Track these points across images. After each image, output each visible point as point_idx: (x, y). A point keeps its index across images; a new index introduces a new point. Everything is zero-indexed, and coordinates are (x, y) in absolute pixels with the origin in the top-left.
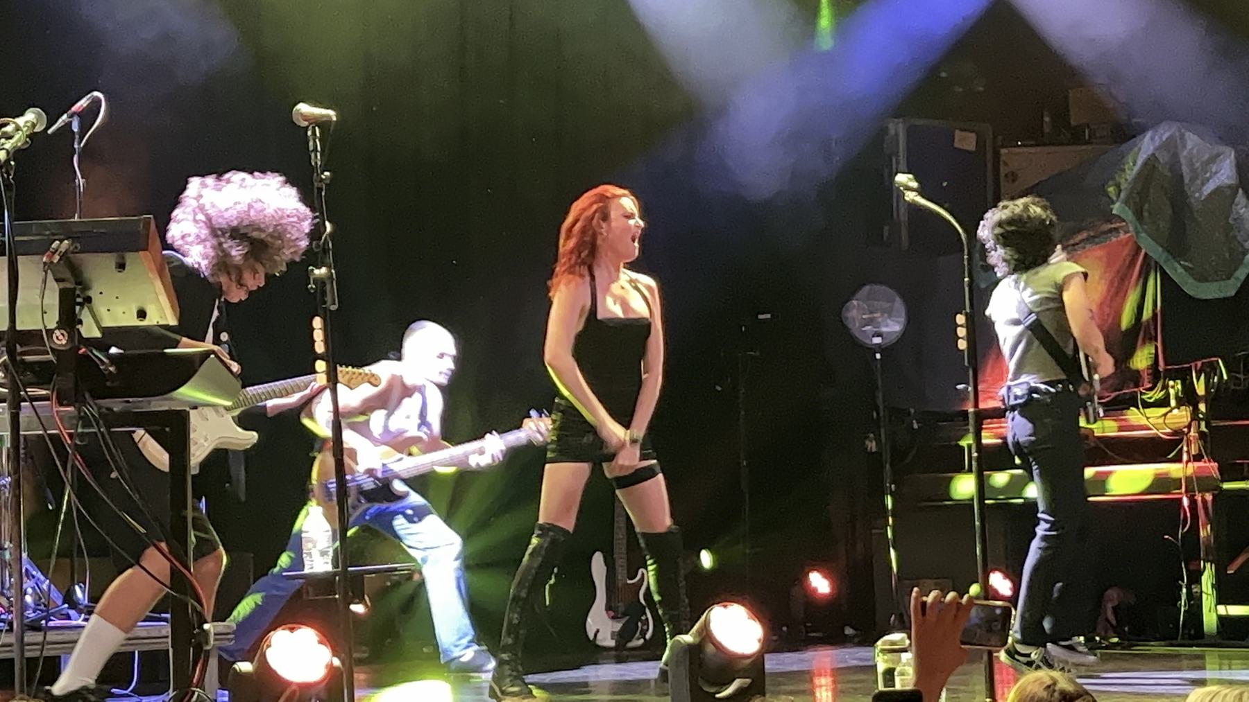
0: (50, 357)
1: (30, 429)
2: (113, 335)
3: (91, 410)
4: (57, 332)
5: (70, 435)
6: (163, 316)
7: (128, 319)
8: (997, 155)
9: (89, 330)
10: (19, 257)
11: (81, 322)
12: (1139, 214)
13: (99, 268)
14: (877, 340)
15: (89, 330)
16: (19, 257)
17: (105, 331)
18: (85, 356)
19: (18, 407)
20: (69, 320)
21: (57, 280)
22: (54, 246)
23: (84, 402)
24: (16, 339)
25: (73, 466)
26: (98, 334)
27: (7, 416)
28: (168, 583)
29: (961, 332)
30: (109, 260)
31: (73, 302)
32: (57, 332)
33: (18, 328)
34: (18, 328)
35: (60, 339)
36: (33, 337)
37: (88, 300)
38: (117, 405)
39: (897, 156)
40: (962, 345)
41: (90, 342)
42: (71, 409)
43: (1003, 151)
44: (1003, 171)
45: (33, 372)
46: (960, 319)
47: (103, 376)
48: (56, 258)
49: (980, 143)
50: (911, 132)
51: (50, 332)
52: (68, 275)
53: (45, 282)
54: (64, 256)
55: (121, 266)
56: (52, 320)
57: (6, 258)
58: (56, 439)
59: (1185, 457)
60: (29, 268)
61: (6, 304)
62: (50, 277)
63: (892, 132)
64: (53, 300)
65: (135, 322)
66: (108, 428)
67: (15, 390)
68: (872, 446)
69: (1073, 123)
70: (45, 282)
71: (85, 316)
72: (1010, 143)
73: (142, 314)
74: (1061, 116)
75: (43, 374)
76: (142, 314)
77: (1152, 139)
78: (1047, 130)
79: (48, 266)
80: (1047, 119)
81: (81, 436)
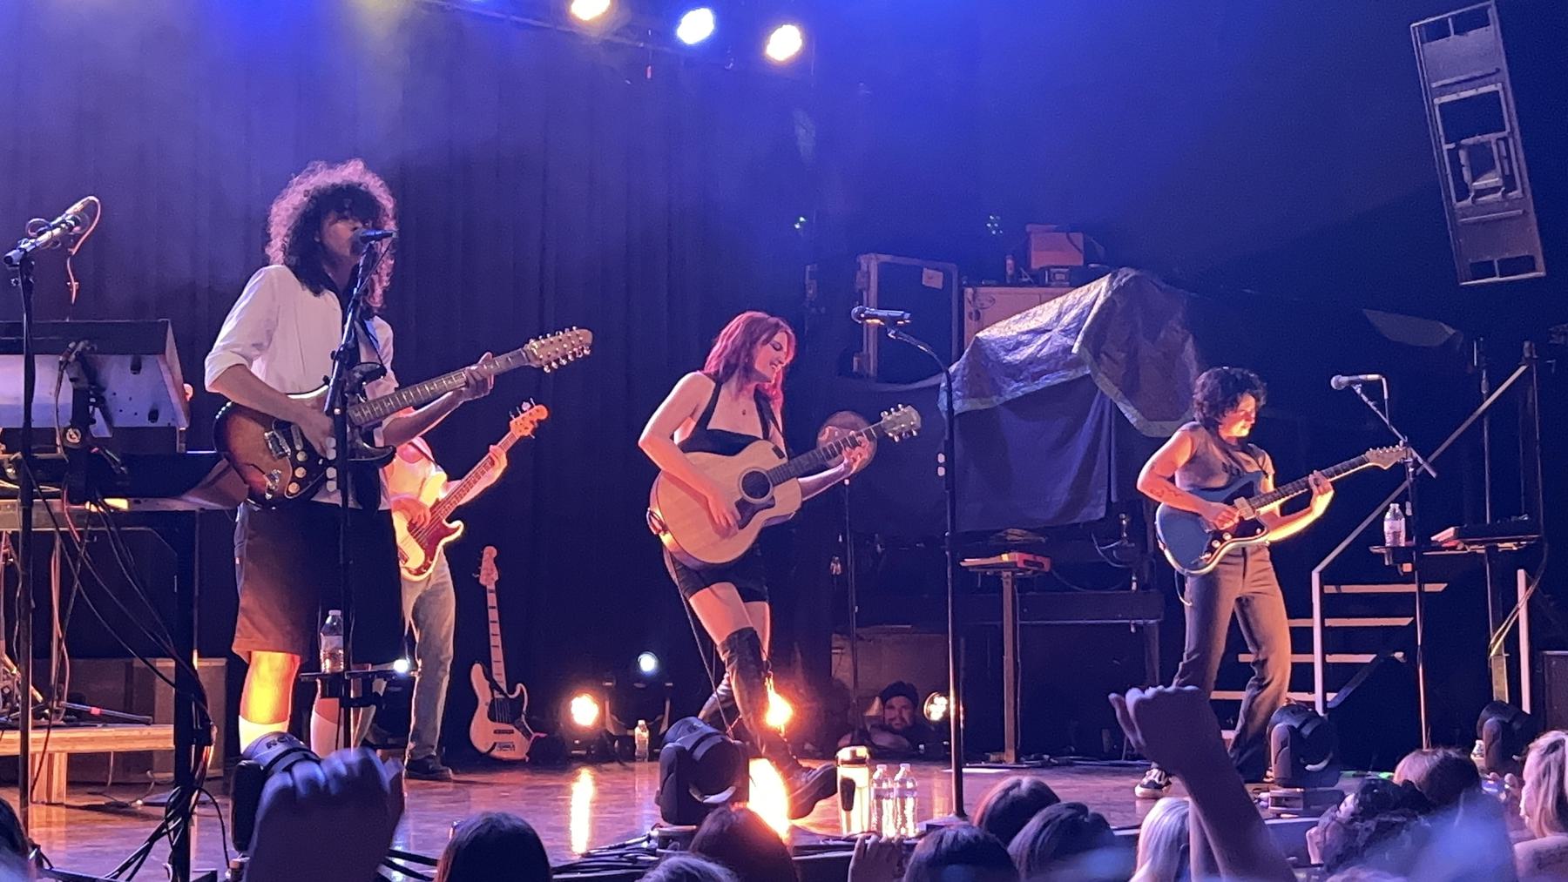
4: (71, 431)
8: (961, 294)
9: (100, 428)
11: (94, 422)
12: (1096, 356)
19: (32, 504)
20: (81, 419)
24: (25, 437)
25: (83, 564)
26: (108, 435)
27: (18, 514)
28: (173, 680)
32: (71, 431)
33: (33, 425)
34: (33, 425)
35: (74, 437)
39: (868, 289)
40: (941, 472)
41: (102, 442)
43: (969, 290)
44: (968, 309)
48: (73, 356)
50: (883, 267)
53: (60, 381)
54: (80, 356)
55: (136, 368)
63: (864, 267)
66: (118, 527)
68: (836, 568)
69: (1035, 266)
70: (60, 381)
72: (976, 281)
73: (153, 415)
74: (1023, 259)
75: (53, 471)
76: (153, 415)
77: (1111, 283)
78: (1010, 272)
79: (64, 366)
80: (1009, 262)
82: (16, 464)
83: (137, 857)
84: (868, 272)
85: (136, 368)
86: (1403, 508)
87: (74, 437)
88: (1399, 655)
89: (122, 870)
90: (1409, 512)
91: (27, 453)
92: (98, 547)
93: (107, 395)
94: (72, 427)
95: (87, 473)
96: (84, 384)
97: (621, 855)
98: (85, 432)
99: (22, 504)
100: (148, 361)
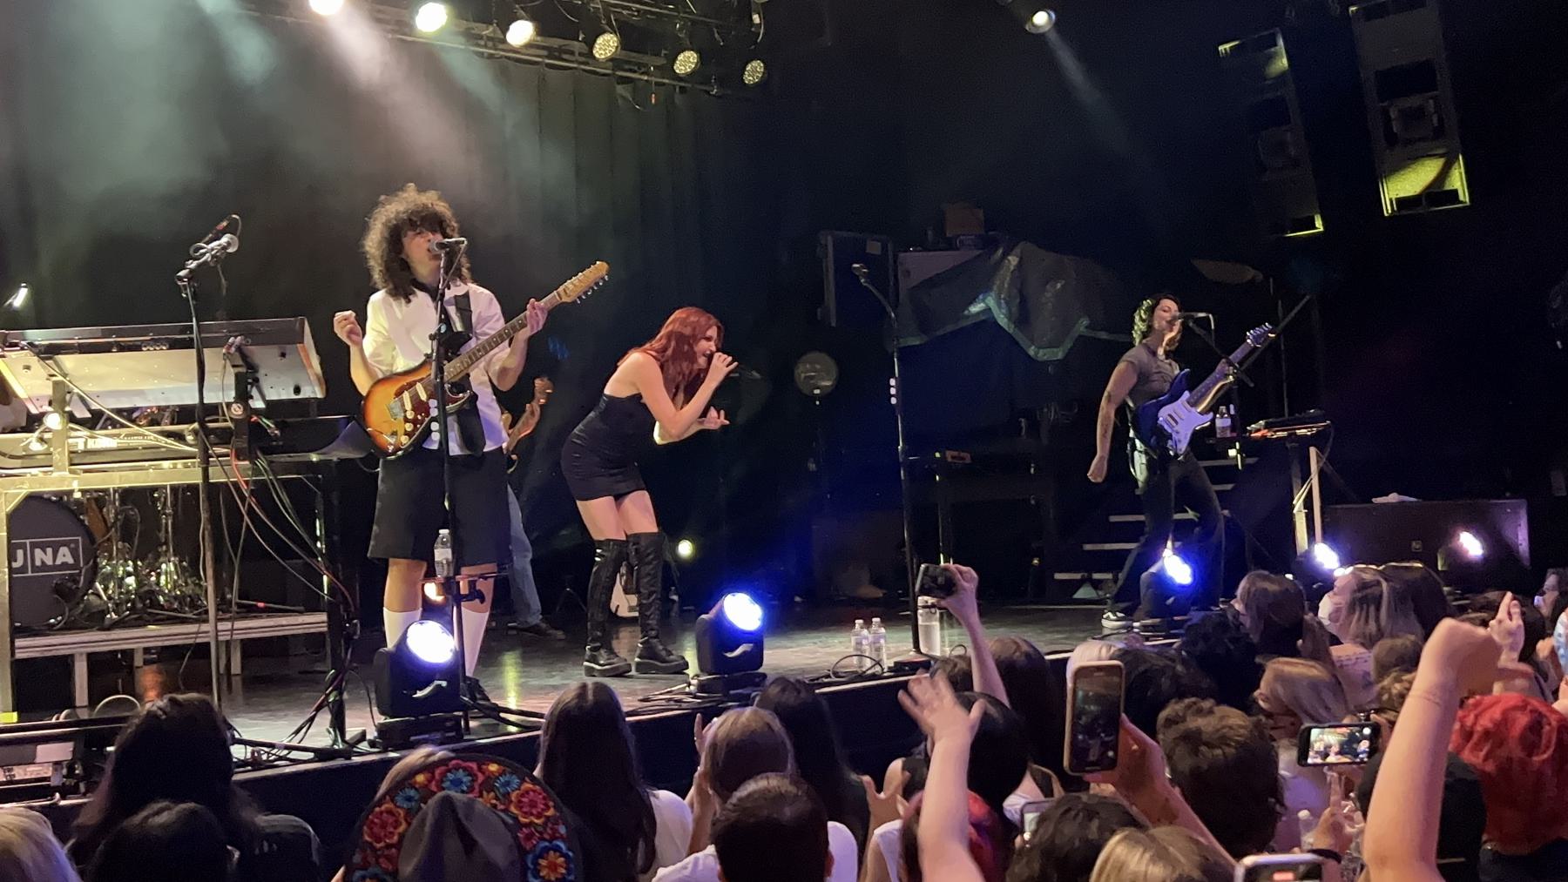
0: (229, 424)
1: (217, 477)
2: (273, 408)
3: (262, 463)
5: (247, 483)
7: (287, 394)
13: (264, 356)
15: (258, 404)
17: (268, 403)
19: (208, 463)
20: (243, 396)
27: (199, 471)
29: (893, 391)
30: (274, 351)
31: (246, 382)
35: (237, 411)
36: (213, 410)
37: (256, 380)
38: (284, 458)
41: (257, 412)
46: (893, 382)
51: (229, 405)
54: (239, 349)
56: (231, 395)
57: (194, 352)
58: (236, 484)
61: (196, 385)
64: (231, 380)
66: (275, 474)
67: (206, 450)
71: (254, 392)
73: (297, 390)
75: (224, 437)
76: (297, 390)
79: (227, 356)
81: (255, 482)
82: (195, 432)
87: (237, 411)
91: (202, 425)
92: (261, 491)
93: (260, 375)
95: (251, 437)
96: (243, 370)
98: (247, 407)
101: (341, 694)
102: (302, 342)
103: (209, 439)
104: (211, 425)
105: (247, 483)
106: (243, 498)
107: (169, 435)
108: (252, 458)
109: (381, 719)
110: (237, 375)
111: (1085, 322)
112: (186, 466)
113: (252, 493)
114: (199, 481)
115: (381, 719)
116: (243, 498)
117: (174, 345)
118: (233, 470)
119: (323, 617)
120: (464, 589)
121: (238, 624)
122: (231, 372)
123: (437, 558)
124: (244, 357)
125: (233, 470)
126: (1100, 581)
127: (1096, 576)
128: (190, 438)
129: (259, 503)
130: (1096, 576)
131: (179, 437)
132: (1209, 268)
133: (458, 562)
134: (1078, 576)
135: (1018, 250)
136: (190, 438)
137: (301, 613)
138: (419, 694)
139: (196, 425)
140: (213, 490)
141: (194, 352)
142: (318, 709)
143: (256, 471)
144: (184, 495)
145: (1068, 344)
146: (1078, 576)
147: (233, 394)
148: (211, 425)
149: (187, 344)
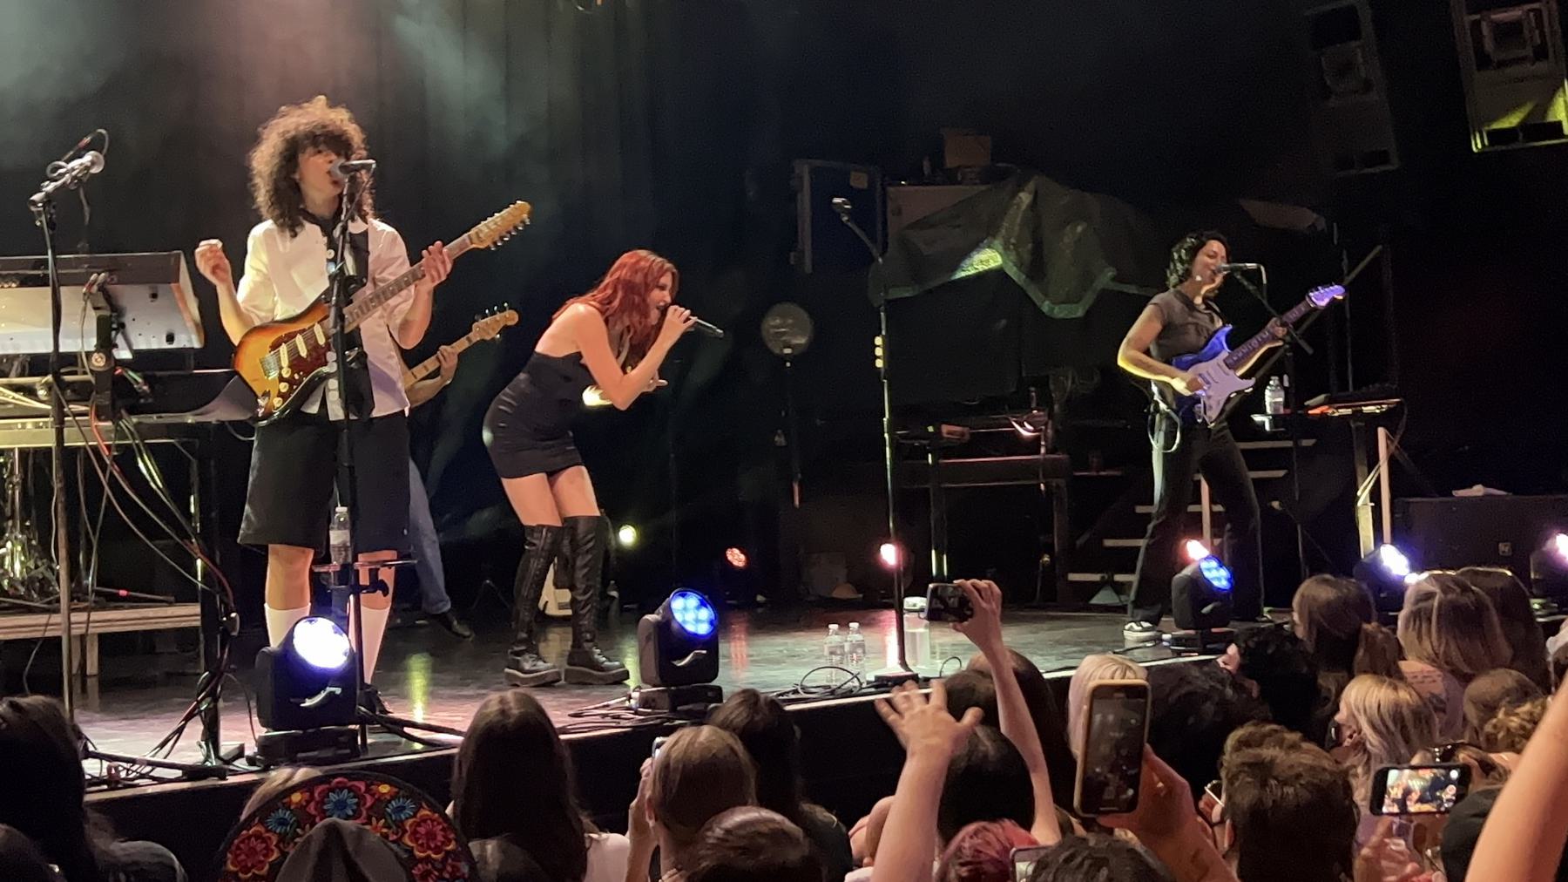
0: (89, 377)
1: (73, 440)
2: (143, 360)
5: (108, 447)
6: (190, 341)
10: (63, 289)
11: (116, 346)
13: (132, 297)
14: (787, 351)
15: (123, 354)
16: (63, 289)
17: (136, 353)
18: (123, 378)
19: (62, 422)
20: (106, 345)
21: (96, 308)
22: (93, 277)
23: (121, 418)
27: (52, 432)
29: (879, 352)
30: (143, 291)
33: (61, 350)
34: (61, 350)
35: (99, 361)
36: (71, 360)
37: (122, 326)
42: (109, 424)
43: (891, 189)
45: (74, 391)
46: (878, 341)
47: (136, 394)
48: (95, 288)
49: (871, 183)
51: (89, 355)
52: (102, 303)
54: (102, 288)
55: (154, 296)
56: (91, 343)
57: (48, 290)
58: (95, 450)
59: (1043, 450)
60: (71, 297)
61: (50, 330)
62: (89, 305)
64: (91, 325)
65: (166, 346)
71: (120, 340)
72: (895, 181)
73: (170, 338)
74: (938, 163)
75: (82, 392)
76: (170, 338)
79: (88, 295)
81: (118, 446)
82: (49, 387)
83: (174, 733)
84: (801, 178)
85: (154, 296)
86: (1281, 381)
87: (99, 361)
88: (1276, 504)
89: (162, 745)
90: (1286, 384)
91: (57, 377)
92: (126, 458)
93: (127, 320)
94: (97, 351)
96: (107, 313)
97: (604, 716)
98: (109, 356)
99: (54, 422)
100: (162, 288)
101: (215, 700)
102: (177, 281)
103: (66, 394)
104: (68, 378)
105: (108, 447)
106: (104, 467)
107: (16, 388)
108: (115, 418)
109: (262, 732)
110: (100, 320)
111: (1110, 273)
112: (37, 426)
113: (115, 459)
114: (52, 444)
115: (262, 732)
116: (104, 467)
117: (25, 282)
118: (91, 432)
119: (196, 609)
120: (364, 580)
121: (95, 616)
122: (92, 316)
123: (333, 542)
124: (109, 298)
125: (91, 432)
126: (1122, 584)
127: (1119, 578)
128: (42, 393)
129: (123, 472)
130: (1119, 578)
131: (30, 391)
132: (1257, 209)
133: (359, 544)
134: (1096, 577)
135: (1031, 185)
136: (42, 393)
137: (170, 604)
138: (308, 703)
139: (49, 378)
140: (69, 455)
141: (48, 290)
142: (188, 719)
143: (120, 434)
144: (35, 460)
145: (1089, 299)
146: (1096, 577)
147: (94, 341)
148: (68, 378)
149: (41, 282)
